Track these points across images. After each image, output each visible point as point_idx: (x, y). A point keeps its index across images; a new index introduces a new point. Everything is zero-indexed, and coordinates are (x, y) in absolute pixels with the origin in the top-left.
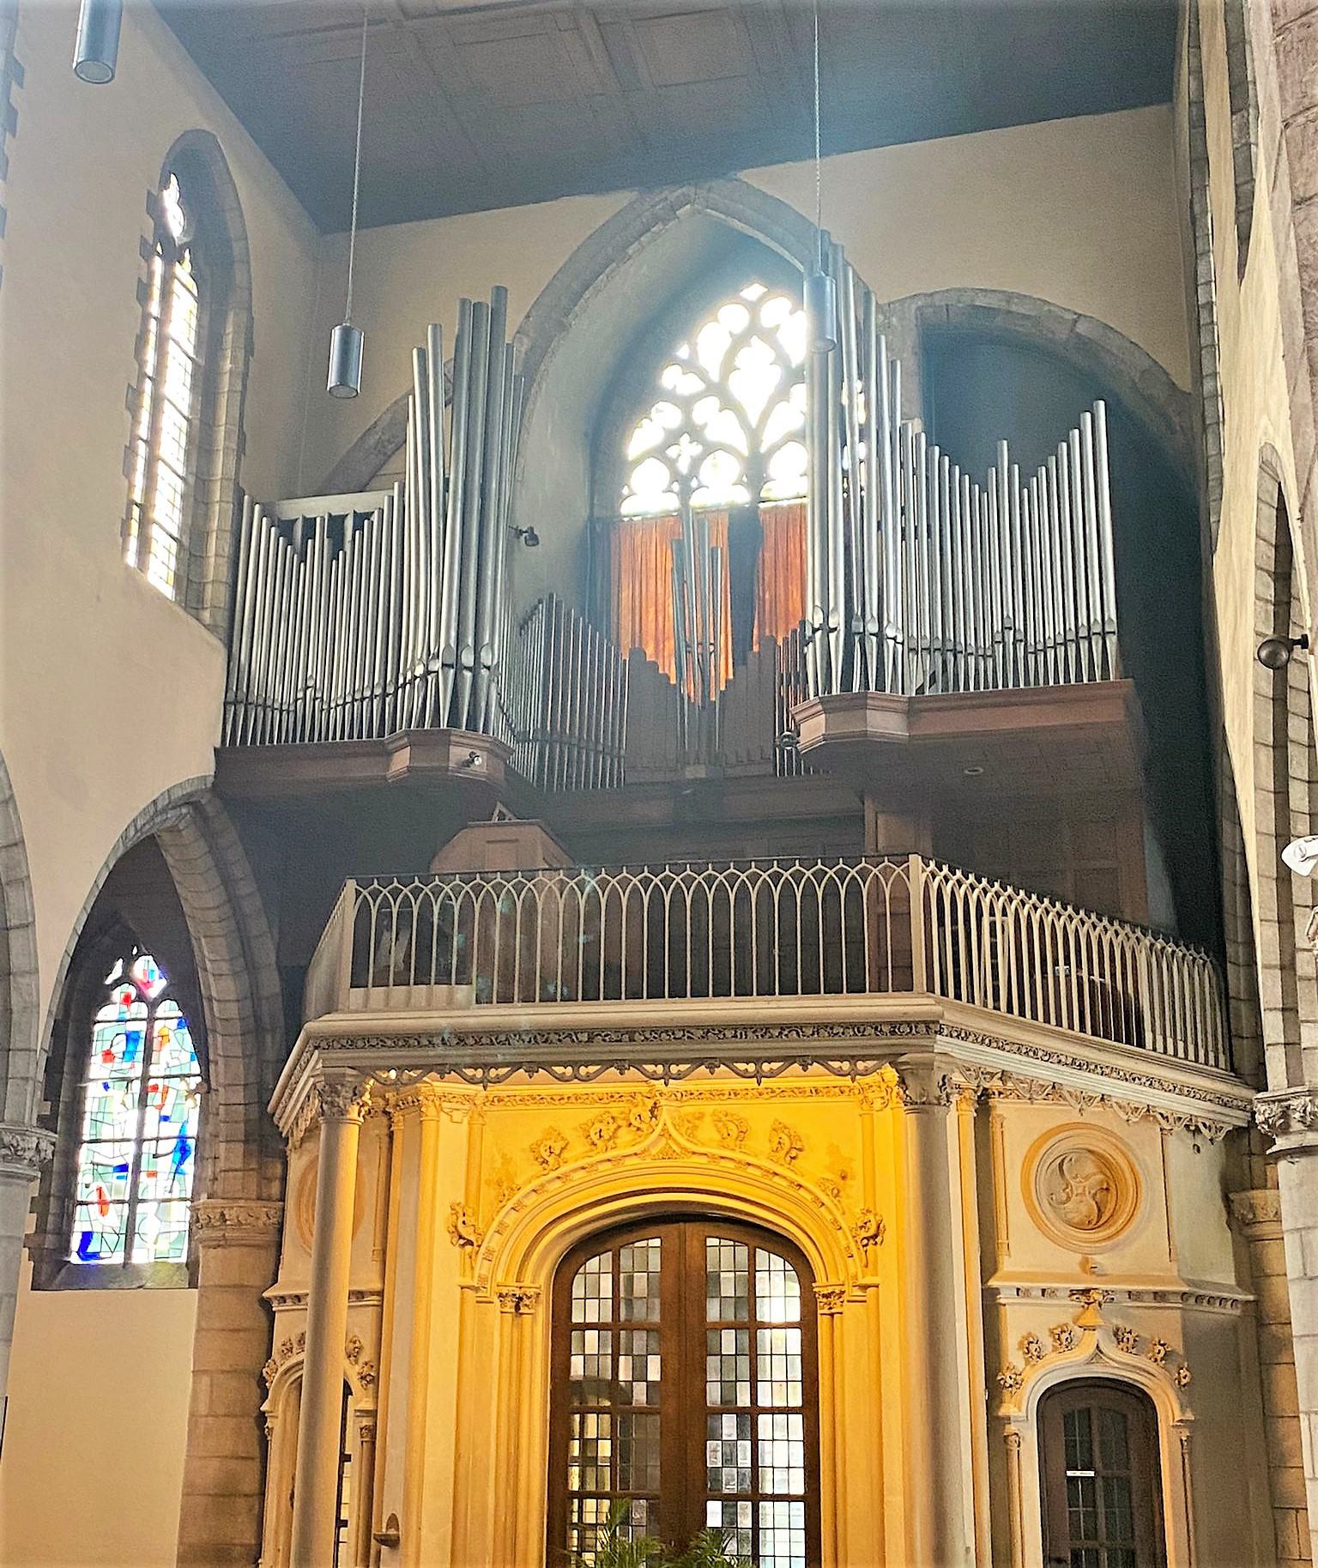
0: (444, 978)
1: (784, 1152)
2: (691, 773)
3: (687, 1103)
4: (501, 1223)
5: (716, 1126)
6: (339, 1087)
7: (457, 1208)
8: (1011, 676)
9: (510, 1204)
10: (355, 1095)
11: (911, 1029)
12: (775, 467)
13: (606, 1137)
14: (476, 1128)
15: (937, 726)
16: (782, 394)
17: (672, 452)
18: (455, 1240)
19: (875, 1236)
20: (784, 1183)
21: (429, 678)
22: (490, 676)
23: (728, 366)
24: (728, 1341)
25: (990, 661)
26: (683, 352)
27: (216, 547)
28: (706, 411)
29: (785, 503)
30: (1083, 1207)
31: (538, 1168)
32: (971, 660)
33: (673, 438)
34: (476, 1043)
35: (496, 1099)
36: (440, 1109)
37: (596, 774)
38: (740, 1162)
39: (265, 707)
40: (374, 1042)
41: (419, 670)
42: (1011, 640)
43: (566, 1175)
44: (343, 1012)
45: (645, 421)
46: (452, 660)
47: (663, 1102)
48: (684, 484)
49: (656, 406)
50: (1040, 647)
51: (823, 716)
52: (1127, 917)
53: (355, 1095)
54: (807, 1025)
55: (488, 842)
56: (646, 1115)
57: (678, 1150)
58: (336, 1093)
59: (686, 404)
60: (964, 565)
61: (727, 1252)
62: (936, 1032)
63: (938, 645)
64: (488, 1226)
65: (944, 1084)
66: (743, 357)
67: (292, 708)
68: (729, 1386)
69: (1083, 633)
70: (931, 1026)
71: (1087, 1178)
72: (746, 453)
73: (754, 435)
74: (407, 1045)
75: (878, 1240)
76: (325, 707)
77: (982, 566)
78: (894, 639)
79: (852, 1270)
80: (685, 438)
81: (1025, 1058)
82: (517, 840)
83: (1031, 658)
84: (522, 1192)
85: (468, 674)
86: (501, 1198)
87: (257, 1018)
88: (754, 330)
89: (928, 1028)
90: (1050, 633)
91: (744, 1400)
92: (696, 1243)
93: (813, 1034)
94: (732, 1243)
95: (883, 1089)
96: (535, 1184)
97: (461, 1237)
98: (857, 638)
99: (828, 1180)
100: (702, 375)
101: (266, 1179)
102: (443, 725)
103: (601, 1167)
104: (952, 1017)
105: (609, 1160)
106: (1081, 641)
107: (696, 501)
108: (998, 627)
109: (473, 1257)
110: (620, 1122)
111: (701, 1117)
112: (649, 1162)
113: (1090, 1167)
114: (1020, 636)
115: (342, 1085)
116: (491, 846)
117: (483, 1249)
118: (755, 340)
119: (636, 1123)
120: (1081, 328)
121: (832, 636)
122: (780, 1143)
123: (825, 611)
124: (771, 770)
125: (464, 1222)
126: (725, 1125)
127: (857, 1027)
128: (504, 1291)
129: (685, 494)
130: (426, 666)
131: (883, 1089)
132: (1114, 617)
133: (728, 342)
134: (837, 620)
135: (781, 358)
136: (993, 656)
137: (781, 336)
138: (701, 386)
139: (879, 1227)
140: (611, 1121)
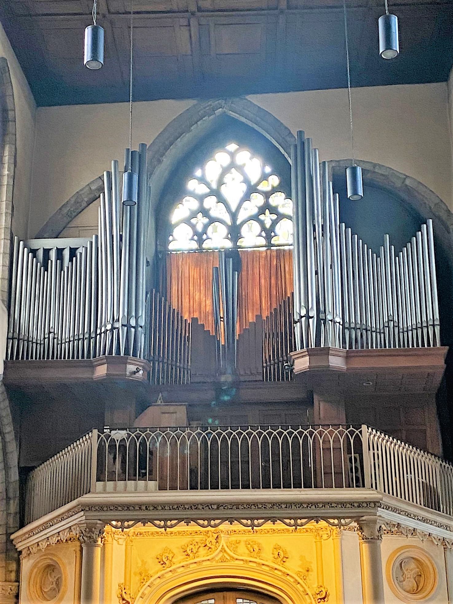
0: (143, 476)
1: (280, 559)
4: (143, 593)
5: (246, 546)
6: (93, 529)
7: (122, 586)
8: (392, 342)
9: (148, 584)
11: (367, 505)
12: (244, 231)
13: (195, 552)
14: (129, 547)
15: (358, 364)
16: (247, 197)
17: (193, 221)
19: (324, 598)
20: (280, 573)
21: (114, 331)
23: (221, 183)
26: (198, 173)
28: (210, 202)
29: (249, 250)
30: (410, 583)
31: (159, 566)
32: (374, 334)
33: (194, 215)
34: (162, 509)
35: (139, 534)
36: (113, 538)
38: (259, 564)
39: (28, 341)
41: (109, 327)
43: (175, 570)
44: (93, 493)
46: (126, 323)
47: (222, 535)
48: (200, 237)
49: (186, 198)
50: (405, 330)
52: (431, 451)
53: (100, 533)
54: (320, 503)
55: (163, 413)
56: (214, 541)
57: (229, 558)
58: (92, 532)
59: (201, 199)
60: (370, 291)
62: (378, 506)
63: (358, 326)
64: (136, 594)
65: (380, 530)
66: (227, 178)
67: (42, 342)
69: (425, 324)
70: (376, 504)
71: (411, 570)
72: (229, 222)
73: (234, 216)
74: (128, 509)
76: (59, 342)
77: (378, 292)
78: (339, 323)
80: (200, 215)
81: (406, 517)
83: (401, 335)
84: (152, 579)
85: (133, 330)
86: (142, 581)
88: (232, 165)
89: (375, 504)
90: (409, 324)
93: (322, 507)
94: (249, 601)
96: (158, 575)
97: (123, 599)
98: (322, 322)
99: (301, 572)
100: (208, 185)
102: (122, 354)
103: (191, 566)
104: (387, 500)
105: (195, 563)
107: (205, 245)
108: (386, 319)
110: (200, 545)
112: (214, 563)
113: (413, 565)
114: (396, 324)
115: (95, 528)
116: (163, 415)
119: (209, 545)
121: (311, 320)
122: (278, 555)
123: (307, 307)
125: (125, 593)
126: (251, 546)
127: (343, 504)
129: (200, 241)
130: (112, 325)
131: (328, 529)
132: (438, 318)
133: (220, 171)
134: (313, 313)
135: (246, 181)
136: (384, 333)
137: (246, 170)
138: (208, 190)
140: (196, 544)
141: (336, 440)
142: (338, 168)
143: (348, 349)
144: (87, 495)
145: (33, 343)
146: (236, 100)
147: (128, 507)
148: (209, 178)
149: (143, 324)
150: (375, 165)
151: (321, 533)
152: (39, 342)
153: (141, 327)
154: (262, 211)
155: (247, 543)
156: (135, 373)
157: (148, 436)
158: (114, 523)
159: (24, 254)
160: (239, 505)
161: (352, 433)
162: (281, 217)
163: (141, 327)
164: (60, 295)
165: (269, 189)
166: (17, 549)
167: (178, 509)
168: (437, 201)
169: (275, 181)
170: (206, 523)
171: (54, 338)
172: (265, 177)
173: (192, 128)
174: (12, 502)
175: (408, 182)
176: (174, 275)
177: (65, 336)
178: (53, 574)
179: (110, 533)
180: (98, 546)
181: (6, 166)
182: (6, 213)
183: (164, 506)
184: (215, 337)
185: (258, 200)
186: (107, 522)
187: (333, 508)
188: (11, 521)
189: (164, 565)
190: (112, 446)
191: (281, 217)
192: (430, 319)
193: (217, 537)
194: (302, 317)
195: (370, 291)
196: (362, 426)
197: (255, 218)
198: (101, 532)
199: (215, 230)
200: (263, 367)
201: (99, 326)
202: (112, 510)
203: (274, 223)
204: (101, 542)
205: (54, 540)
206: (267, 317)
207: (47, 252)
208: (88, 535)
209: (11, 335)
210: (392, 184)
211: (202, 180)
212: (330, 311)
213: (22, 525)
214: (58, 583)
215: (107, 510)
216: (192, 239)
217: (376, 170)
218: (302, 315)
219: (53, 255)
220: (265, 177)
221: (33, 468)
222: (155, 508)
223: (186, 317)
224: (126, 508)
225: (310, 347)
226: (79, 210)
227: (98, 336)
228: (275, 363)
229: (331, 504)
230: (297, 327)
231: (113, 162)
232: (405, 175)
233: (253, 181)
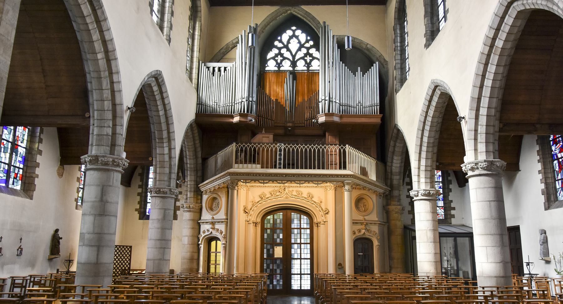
0: (254, 162)
8: (360, 112)
12: (298, 63)
15: (345, 120)
16: (299, 49)
17: (276, 58)
23: (288, 42)
25: (356, 109)
26: (279, 38)
28: (284, 51)
33: (276, 55)
37: (268, 123)
41: (240, 101)
45: (271, 52)
48: (279, 65)
59: (280, 49)
66: (291, 41)
72: (292, 60)
73: (294, 57)
74: (248, 175)
77: (354, 90)
80: (279, 56)
83: (363, 109)
85: (251, 102)
87: (197, 168)
88: (294, 36)
97: (245, 212)
100: (283, 43)
101: (197, 199)
103: (273, 199)
108: (357, 102)
111: (293, 191)
114: (362, 105)
117: (250, 214)
118: (294, 38)
120: (368, 46)
121: (326, 101)
129: (279, 67)
134: (327, 98)
135: (299, 42)
137: (300, 38)
141: (336, 151)
144: (231, 169)
146: (297, 7)
149: (255, 100)
151: (327, 188)
153: (254, 101)
154: (306, 55)
155: (297, 191)
157: (257, 146)
158: (242, 181)
161: (342, 148)
163: (254, 101)
165: (309, 46)
169: (311, 43)
172: (307, 41)
176: (268, 81)
178: (216, 201)
180: (236, 189)
185: (304, 51)
186: (239, 180)
188: (198, 180)
190: (242, 150)
191: (314, 58)
194: (322, 100)
197: (302, 58)
198: (237, 184)
199: (285, 63)
203: (311, 61)
205: (217, 187)
207: (214, 68)
211: (281, 41)
213: (203, 181)
214: (218, 204)
219: (216, 69)
220: (307, 41)
221: (207, 158)
222: (260, 175)
223: (272, 99)
227: (235, 105)
228: (310, 119)
230: (320, 104)
231: (243, 31)
233: (303, 42)
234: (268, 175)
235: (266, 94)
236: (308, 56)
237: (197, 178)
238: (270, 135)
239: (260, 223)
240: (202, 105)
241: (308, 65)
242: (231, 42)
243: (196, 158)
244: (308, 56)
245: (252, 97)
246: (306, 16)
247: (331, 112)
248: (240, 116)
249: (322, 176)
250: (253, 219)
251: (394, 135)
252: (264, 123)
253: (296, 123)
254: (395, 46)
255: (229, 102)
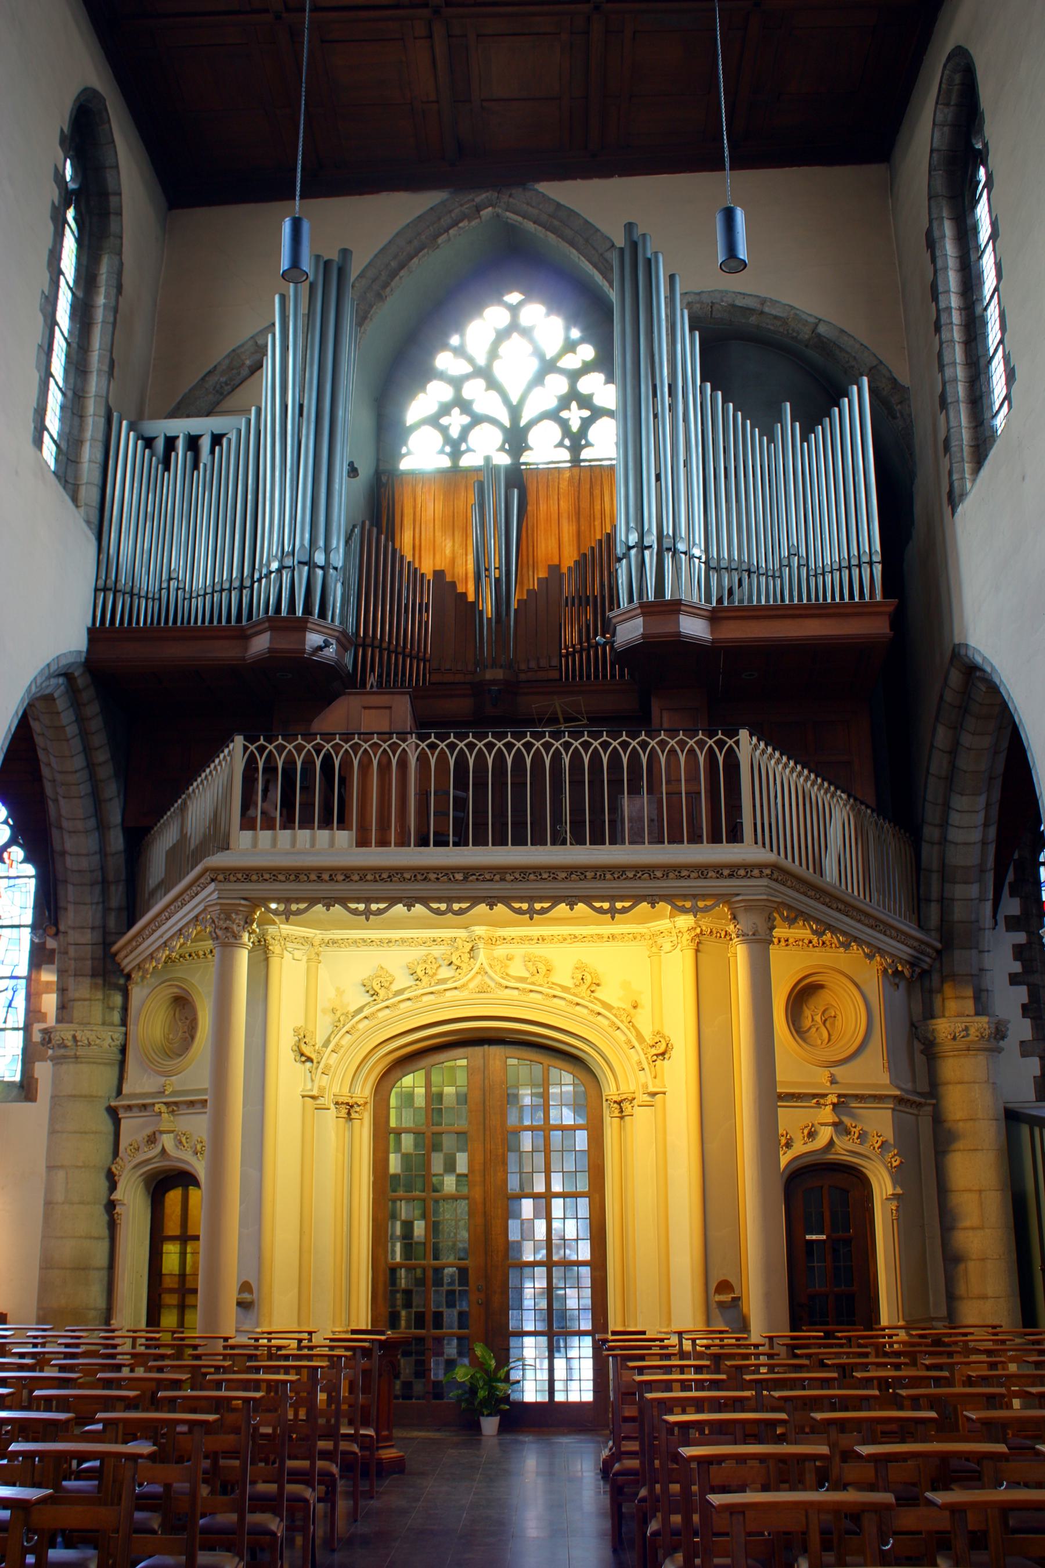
0: (326, 823)
1: (585, 987)
2: (489, 675)
3: (500, 947)
5: (525, 965)
8: (795, 594)
10: (246, 923)
12: (533, 438)
16: (539, 379)
17: (444, 421)
18: (298, 1058)
22: (337, 576)
23: (493, 354)
24: (527, 1142)
25: (778, 581)
26: (455, 340)
27: (90, 454)
32: (763, 579)
33: (445, 410)
34: (361, 879)
35: (330, 942)
38: (547, 995)
40: (267, 876)
41: (275, 566)
42: (796, 565)
43: (394, 1005)
46: (305, 559)
47: (481, 945)
48: (455, 447)
51: (641, 619)
53: (246, 923)
55: (365, 708)
57: (492, 984)
58: (230, 920)
59: (457, 383)
61: (524, 1072)
66: (504, 349)
67: (157, 596)
68: (526, 1179)
69: (854, 562)
72: (507, 424)
73: (515, 412)
75: (666, 1056)
76: (187, 596)
77: (771, 505)
78: (699, 558)
79: (643, 1080)
80: (456, 411)
82: (390, 708)
85: (320, 572)
87: (103, 869)
88: (514, 327)
91: (540, 1187)
92: (498, 1062)
94: (529, 1062)
95: (674, 934)
97: (302, 1055)
100: (471, 360)
102: (299, 612)
103: (425, 999)
106: (853, 568)
107: (465, 462)
109: (314, 1071)
110: (441, 962)
111: (509, 958)
115: (237, 914)
116: (367, 711)
117: (322, 1065)
119: (456, 962)
122: (582, 979)
124: (557, 677)
126: (533, 965)
128: (341, 1100)
129: (456, 454)
130: (281, 561)
131: (674, 934)
132: (878, 549)
133: (492, 336)
134: (651, 539)
136: (781, 577)
137: (537, 334)
138: (468, 369)
139: (667, 1044)
142: (698, 305)
143: (714, 604)
145: (139, 597)
147: (296, 874)
148: (471, 349)
149: (340, 564)
150: (763, 301)
151: (660, 941)
152: (150, 595)
153: (336, 569)
154: (565, 402)
155: (528, 960)
156: (320, 648)
157: (337, 747)
158: (273, 906)
159: (128, 442)
160: (506, 873)
161: (720, 744)
162: (598, 413)
163: (336, 569)
164: (190, 515)
165: (578, 365)
166: (123, 970)
167: (391, 881)
168: (875, 363)
169: (587, 352)
170: (443, 906)
171: (184, 599)
172: (570, 347)
173: (440, 240)
174: (113, 888)
175: (822, 329)
177: (199, 583)
179: (277, 938)
180: (243, 946)
181: (102, 290)
182: (99, 371)
183: (363, 874)
184: (474, 605)
185: (557, 385)
187: (682, 879)
188: (112, 923)
189: (375, 997)
190: (270, 769)
191: (598, 413)
192: (865, 552)
193: (472, 949)
194: (630, 548)
195: (757, 502)
196: (741, 731)
197: (553, 415)
200: (561, 655)
201: (257, 567)
202: (266, 880)
203: (586, 423)
204: (249, 940)
206: (569, 568)
207: (170, 443)
208: (225, 926)
209: (101, 583)
210: (795, 334)
212: (683, 536)
215: (257, 881)
216: (442, 452)
217: (766, 310)
218: (631, 544)
220: (570, 347)
222: (347, 878)
224: (292, 877)
225: (645, 600)
226: (236, 382)
227: (256, 585)
229: (679, 872)
232: (816, 318)
234: (385, 876)
235: (402, 557)
236: (574, 405)
237: (104, 917)
238: (397, 697)
239: (370, 1107)
240: (116, 592)
241: (576, 441)
242: (251, 343)
243: (102, 827)
244: (574, 405)
245: (327, 550)
246: (556, 223)
247: (668, 597)
248: (272, 629)
249: (630, 875)
250: (335, 1089)
251: (949, 697)
252: (388, 675)
253: (523, 667)
254: (938, 311)
255: (230, 572)
